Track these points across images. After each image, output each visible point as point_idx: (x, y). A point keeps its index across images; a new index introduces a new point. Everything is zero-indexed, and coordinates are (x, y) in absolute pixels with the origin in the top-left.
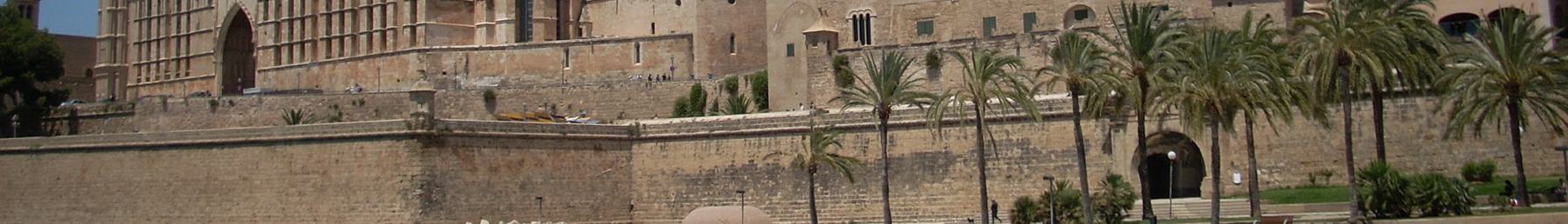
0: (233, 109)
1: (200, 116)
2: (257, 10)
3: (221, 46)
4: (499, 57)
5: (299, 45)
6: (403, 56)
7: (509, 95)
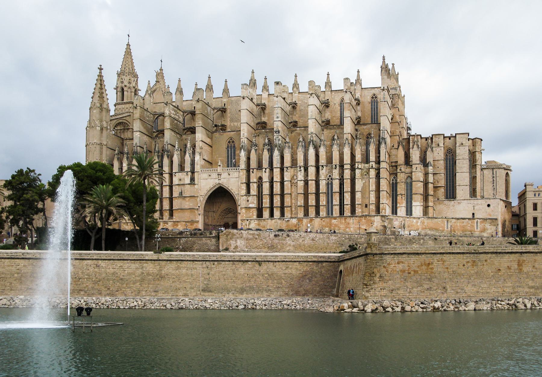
0: (288, 238)
1: (265, 241)
2: (239, 188)
3: (203, 206)
4: (417, 222)
5: (279, 209)
6: (370, 218)
7: (445, 239)
